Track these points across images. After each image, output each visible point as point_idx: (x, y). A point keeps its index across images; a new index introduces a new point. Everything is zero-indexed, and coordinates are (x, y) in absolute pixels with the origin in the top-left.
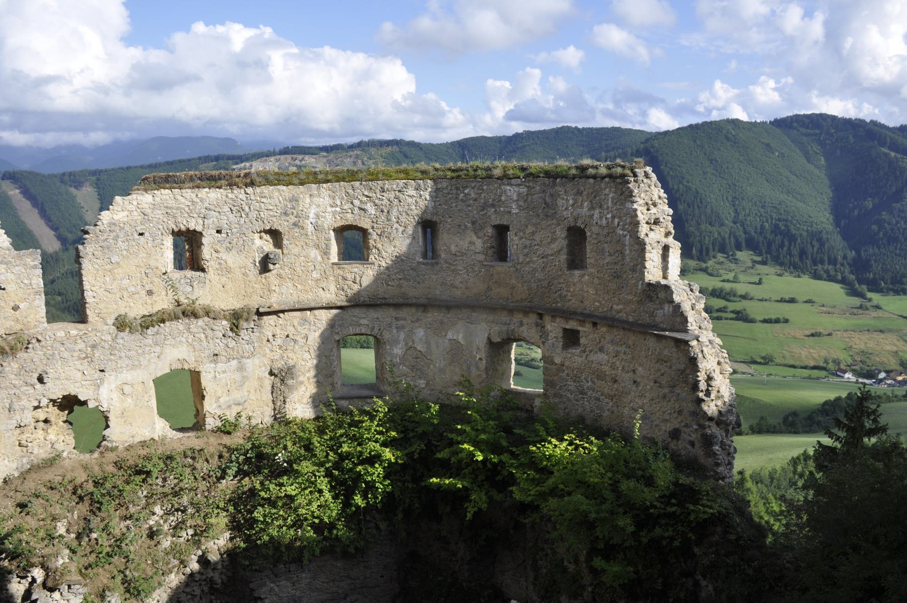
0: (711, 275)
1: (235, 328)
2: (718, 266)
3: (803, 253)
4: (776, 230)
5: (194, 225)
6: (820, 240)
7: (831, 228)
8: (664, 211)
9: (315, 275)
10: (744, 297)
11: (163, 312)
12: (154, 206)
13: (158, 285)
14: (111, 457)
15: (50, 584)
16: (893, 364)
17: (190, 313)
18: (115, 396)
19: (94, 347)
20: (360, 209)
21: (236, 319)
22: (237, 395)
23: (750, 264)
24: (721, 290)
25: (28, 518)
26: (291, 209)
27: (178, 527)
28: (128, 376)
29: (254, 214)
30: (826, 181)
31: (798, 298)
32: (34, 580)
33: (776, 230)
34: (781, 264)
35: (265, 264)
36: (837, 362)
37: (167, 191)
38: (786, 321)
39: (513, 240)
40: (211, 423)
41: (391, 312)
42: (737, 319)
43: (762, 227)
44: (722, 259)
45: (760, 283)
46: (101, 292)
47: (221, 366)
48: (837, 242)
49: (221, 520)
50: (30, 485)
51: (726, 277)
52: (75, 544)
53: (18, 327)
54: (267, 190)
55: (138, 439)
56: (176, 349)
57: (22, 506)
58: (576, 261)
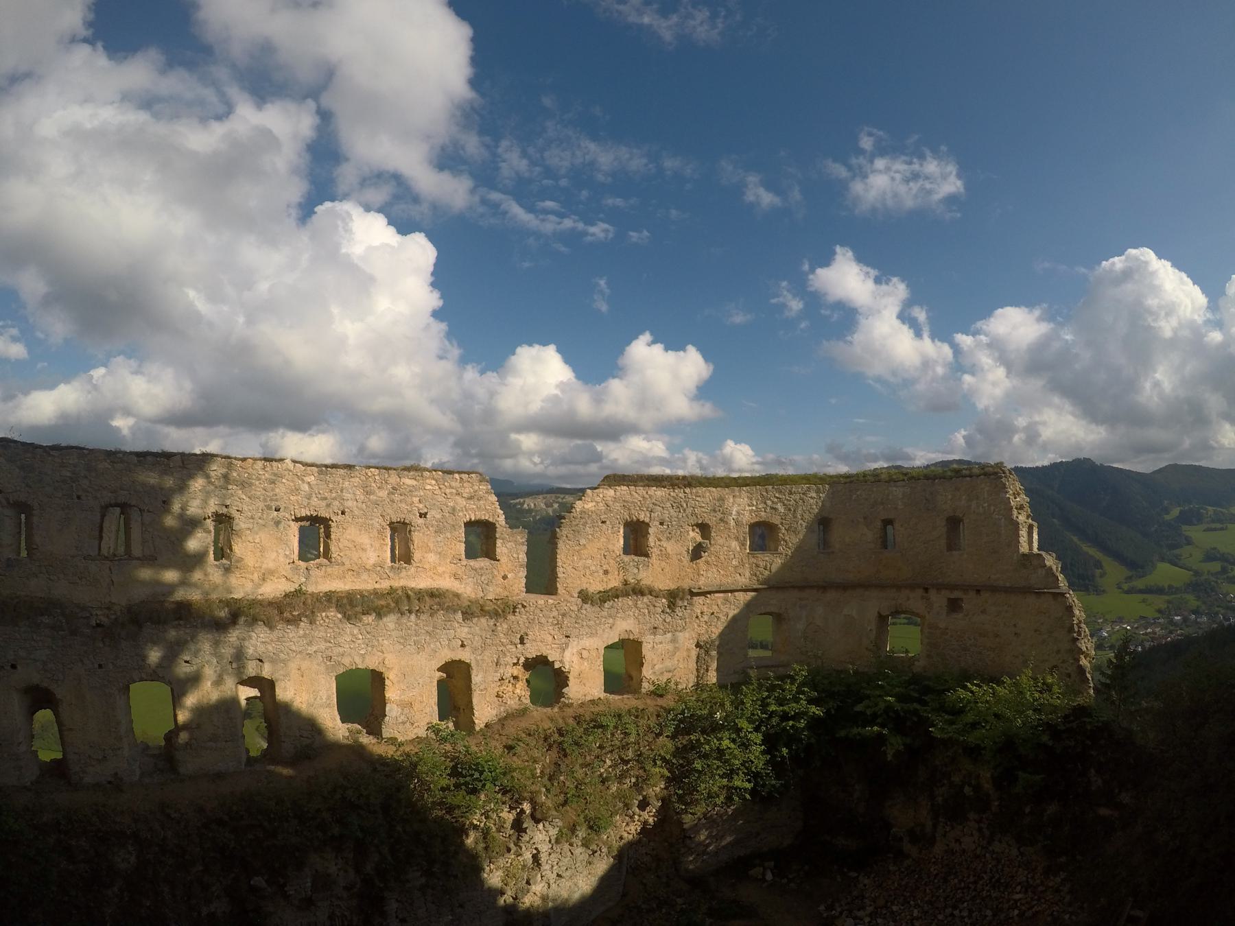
1: (672, 606)
5: (643, 517)
8: (1023, 499)
9: (734, 562)
11: (615, 589)
12: (615, 499)
13: (612, 566)
14: (570, 712)
15: (538, 816)
17: (638, 591)
18: (576, 659)
19: (564, 615)
20: (772, 508)
21: (673, 597)
22: (668, 664)
25: (515, 758)
26: (719, 508)
27: (621, 778)
28: (588, 642)
29: (689, 510)
32: (523, 811)
35: (697, 553)
37: (625, 488)
40: (646, 687)
46: (569, 569)
47: (659, 638)
49: (659, 770)
50: (511, 729)
52: (548, 784)
53: (506, 593)
54: (701, 490)
55: (589, 698)
56: (624, 622)
57: (510, 748)
58: (952, 545)
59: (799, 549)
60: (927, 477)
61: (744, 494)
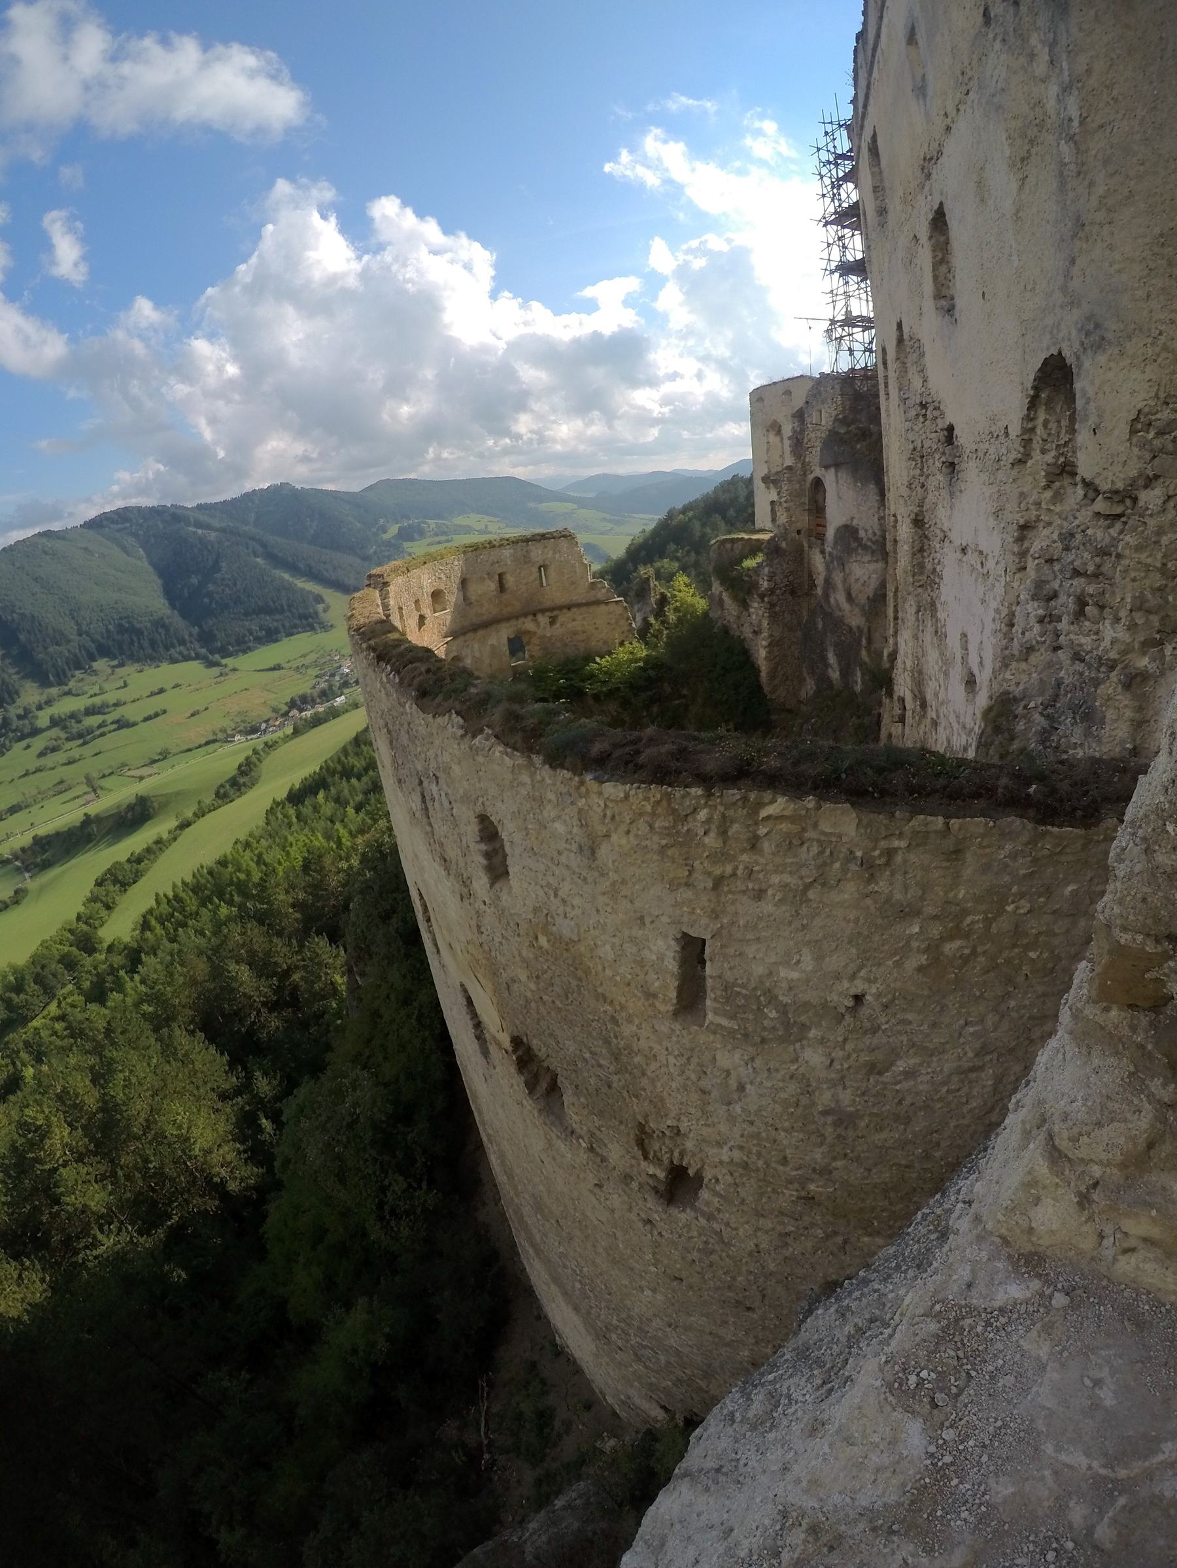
0: (78, 695)
2: (80, 684)
3: (153, 644)
4: (121, 629)
6: (164, 626)
7: (169, 612)
10: (116, 705)
16: (269, 714)
23: (109, 671)
24: (94, 706)
30: (151, 569)
31: (166, 686)
33: (121, 629)
34: (138, 660)
36: (224, 730)
38: (165, 712)
39: (510, 580)
41: (462, 638)
42: (119, 728)
43: (108, 631)
44: (81, 676)
45: (125, 685)
48: (178, 622)
51: (91, 692)
59: (455, 604)
60: (523, 541)
61: (426, 571)
